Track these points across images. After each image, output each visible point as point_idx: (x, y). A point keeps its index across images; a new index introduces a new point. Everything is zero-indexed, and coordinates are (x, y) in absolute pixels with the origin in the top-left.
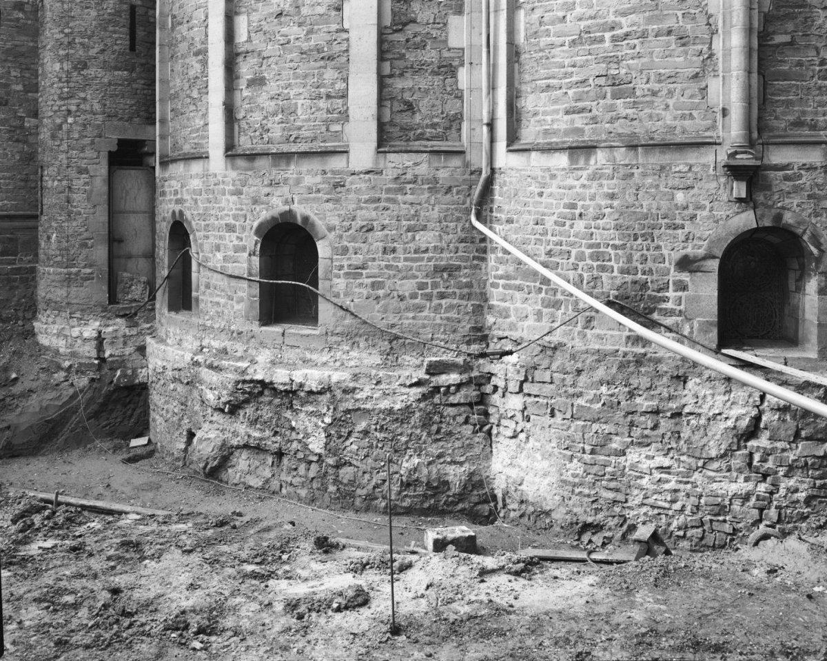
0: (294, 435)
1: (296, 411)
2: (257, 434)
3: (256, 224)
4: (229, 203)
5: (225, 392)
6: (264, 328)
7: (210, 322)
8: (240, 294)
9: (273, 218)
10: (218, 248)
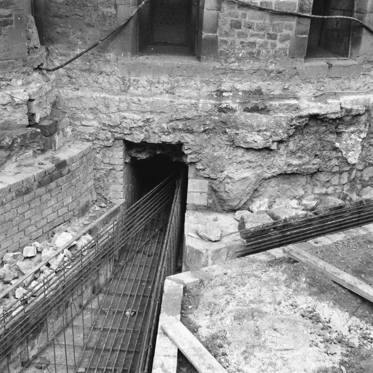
0: (334, 154)
1: (339, 134)
2: (296, 162)
5: (281, 131)
6: (307, 64)
7: (237, 64)
8: (286, 32)
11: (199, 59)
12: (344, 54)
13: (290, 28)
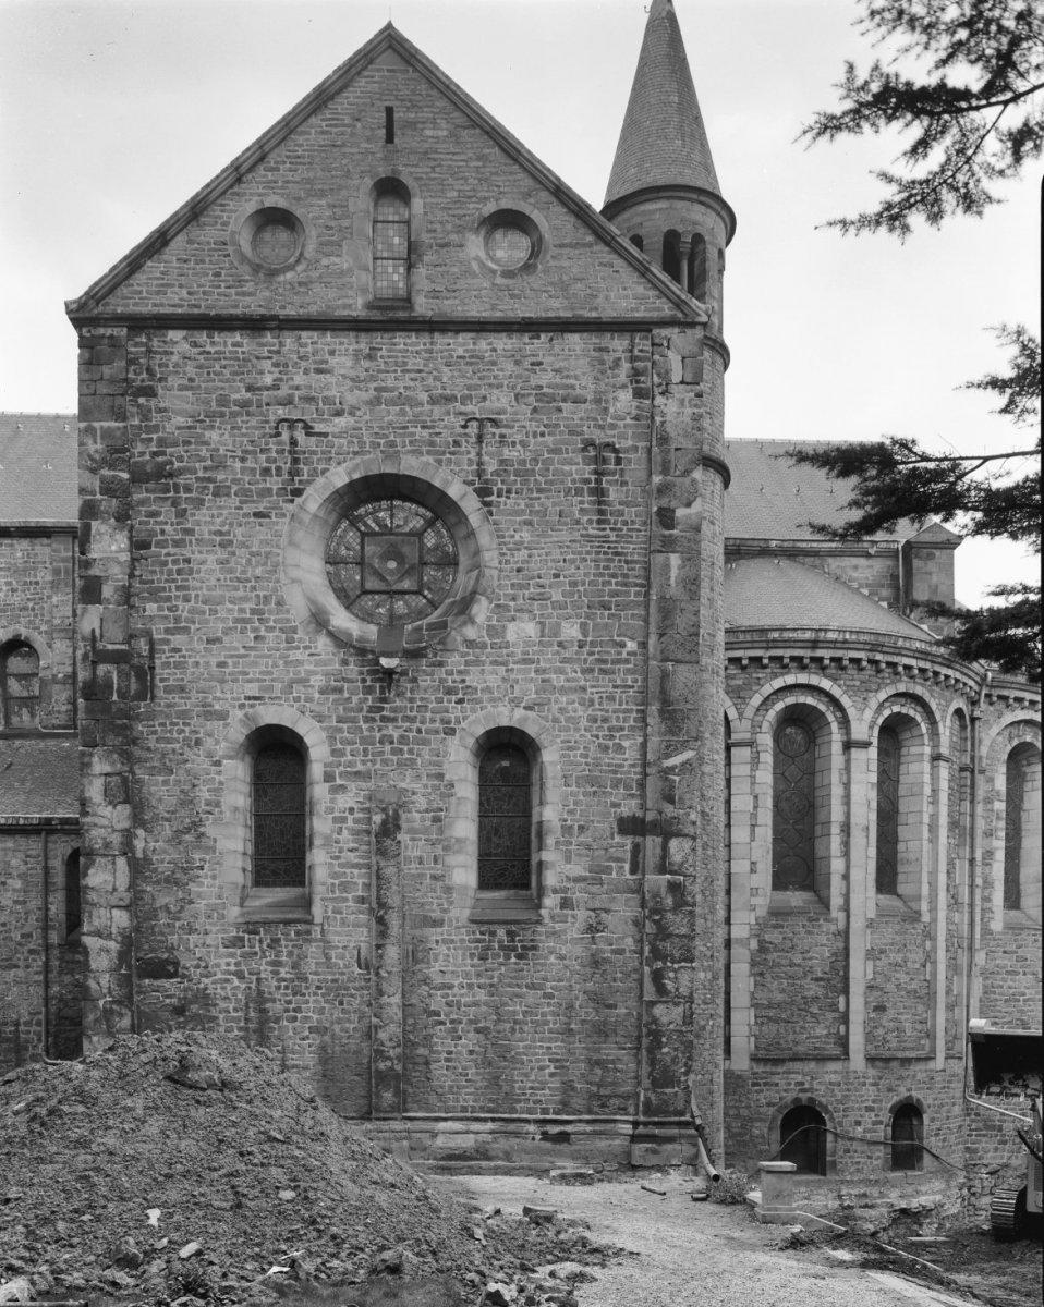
1: (921, 1225)
3: (889, 1105)
4: (870, 1092)
8: (877, 1154)
9: (901, 1101)
10: (858, 1123)
11: (825, 1175)
12: (913, 1168)
13: (881, 1153)
